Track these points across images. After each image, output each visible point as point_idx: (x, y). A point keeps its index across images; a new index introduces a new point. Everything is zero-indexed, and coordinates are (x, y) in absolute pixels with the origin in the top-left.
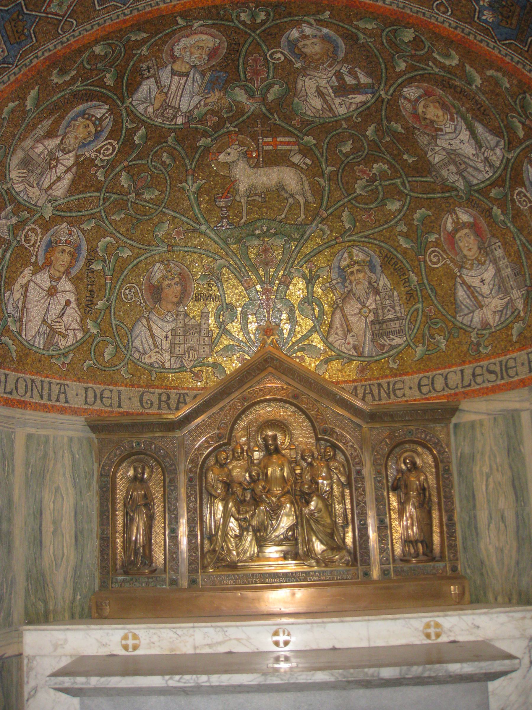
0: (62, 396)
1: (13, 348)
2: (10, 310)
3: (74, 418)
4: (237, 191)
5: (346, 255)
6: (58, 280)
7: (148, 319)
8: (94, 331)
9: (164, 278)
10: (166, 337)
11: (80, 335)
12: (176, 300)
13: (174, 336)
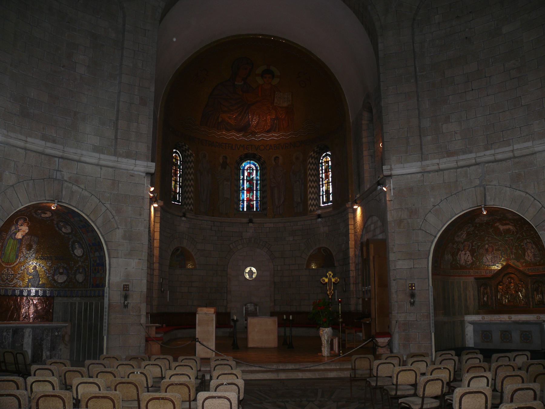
0: (469, 273)
1: (459, 266)
2: (458, 259)
3: (472, 277)
4: (501, 230)
5: (526, 241)
6: (466, 252)
7: (486, 256)
8: (475, 260)
9: (488, 247)
10: (490, 259)
11: (472, 261)
12: (491, 251)
13: (492, 259)
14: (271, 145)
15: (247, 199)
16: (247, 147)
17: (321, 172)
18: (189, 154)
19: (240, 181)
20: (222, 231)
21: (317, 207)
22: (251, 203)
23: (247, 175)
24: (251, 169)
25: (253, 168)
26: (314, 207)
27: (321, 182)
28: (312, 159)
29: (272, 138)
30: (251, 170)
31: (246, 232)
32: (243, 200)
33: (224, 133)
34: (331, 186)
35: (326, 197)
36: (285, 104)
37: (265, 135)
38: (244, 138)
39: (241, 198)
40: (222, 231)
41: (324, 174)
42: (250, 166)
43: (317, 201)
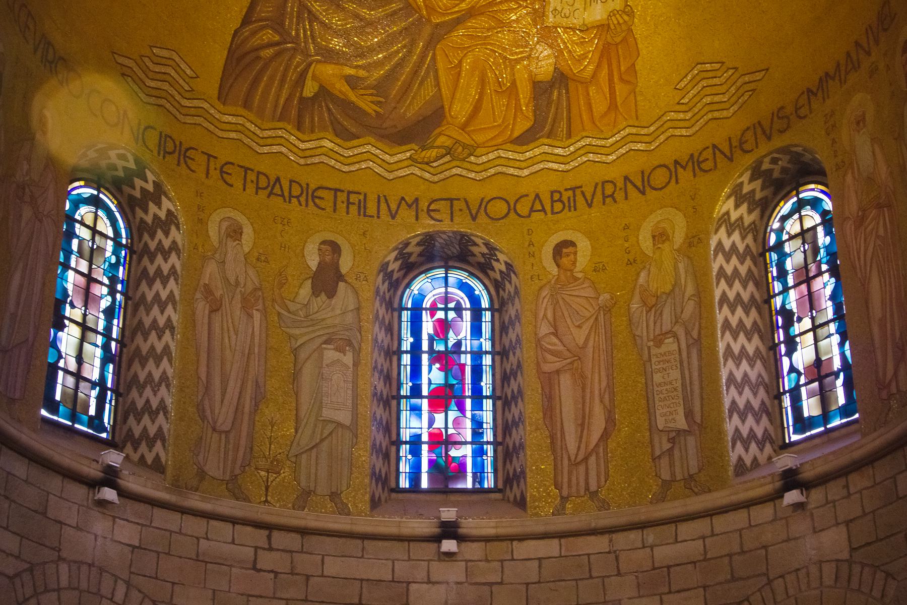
14: (537, 196)
15: (431, 435)
16: (432, 207)
17: (778, 287)
18: (162, 215)
19: (399, 360)
20: (308, 577)
21: (768, 449)
22: (453, 453)
23: (431, 332)
24: (452, 305)
25: (458, 303)
26: (753, 446)
27: (781, 331)
28: (729, 235)
29: (541, 166)
30: (451, 309)
31: (429, 582)
32: (415, 442)
33: (327, 144)
34: (836, 339)
35: (810, 395)
36: (597, 13)
37: (510, 155)
38: (418, 172)
39: (406, 435)
40: (308, 577)
41: (793, 295)
42: (447, 293)
43: (770, 420)
